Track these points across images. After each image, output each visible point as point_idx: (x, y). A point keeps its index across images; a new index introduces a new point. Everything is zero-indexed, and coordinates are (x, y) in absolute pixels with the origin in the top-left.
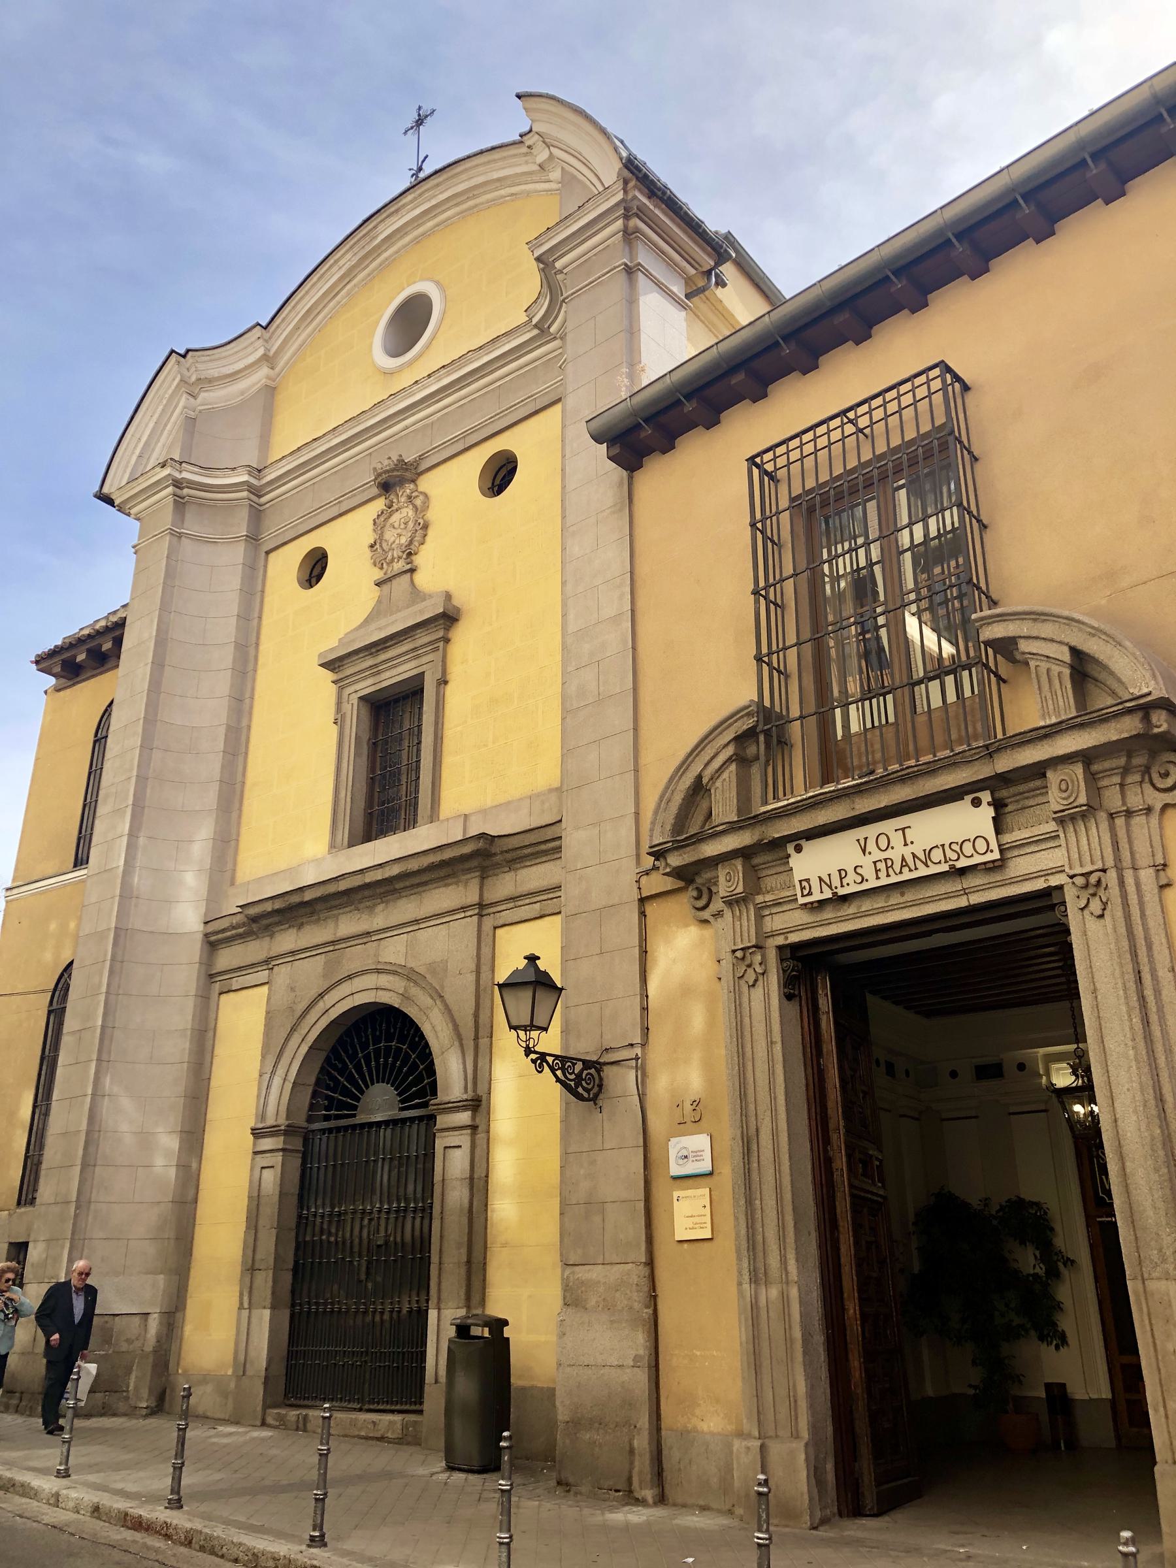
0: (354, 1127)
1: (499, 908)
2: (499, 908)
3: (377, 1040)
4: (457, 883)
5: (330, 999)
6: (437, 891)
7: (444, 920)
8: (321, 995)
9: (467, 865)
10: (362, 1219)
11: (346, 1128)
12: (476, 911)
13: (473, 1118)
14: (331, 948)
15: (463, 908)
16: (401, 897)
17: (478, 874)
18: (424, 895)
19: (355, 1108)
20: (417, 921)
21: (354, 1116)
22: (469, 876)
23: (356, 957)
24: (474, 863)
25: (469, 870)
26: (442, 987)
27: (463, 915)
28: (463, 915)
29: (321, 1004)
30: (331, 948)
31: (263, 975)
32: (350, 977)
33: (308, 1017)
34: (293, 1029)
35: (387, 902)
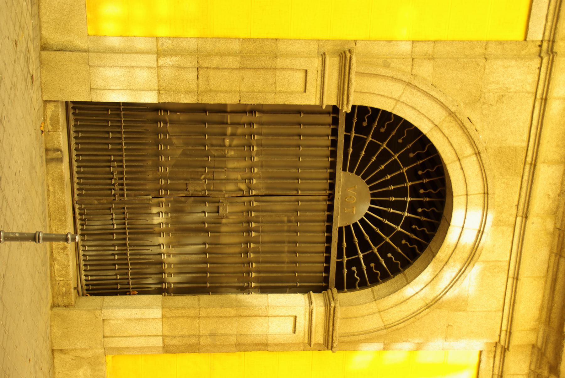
0: (333, 165)
1: (498, 358)
2: (498, 358)
3: (414, 191)
4: (539, 319)
5: (471, 164)
6: (540, 296)
7: (507, 307)
8: (478, 154)
9: (551, 347)
10: (244, 179)
11: (334, 154)
12: (502, 343)
13: (318, 344)
14: (529, 159)
15: (510, 333)
16: (551, 252)
17: (539, 344)
18: (542, 281)
19: (351, 171)
20: (516, 278)
21: (344, 169)
22: (541, 334)
23: (506, 191)
24: (550, 353)
25: (546, 340)
26: (440, 308)
27: (504, 328)
28: (504, 328)
29: (469, 151)
30: (529, 159)
31: (537, 34)
32: (486, 193)
33: (460, 132)
34: (452, 114)
35: (553, 234)
